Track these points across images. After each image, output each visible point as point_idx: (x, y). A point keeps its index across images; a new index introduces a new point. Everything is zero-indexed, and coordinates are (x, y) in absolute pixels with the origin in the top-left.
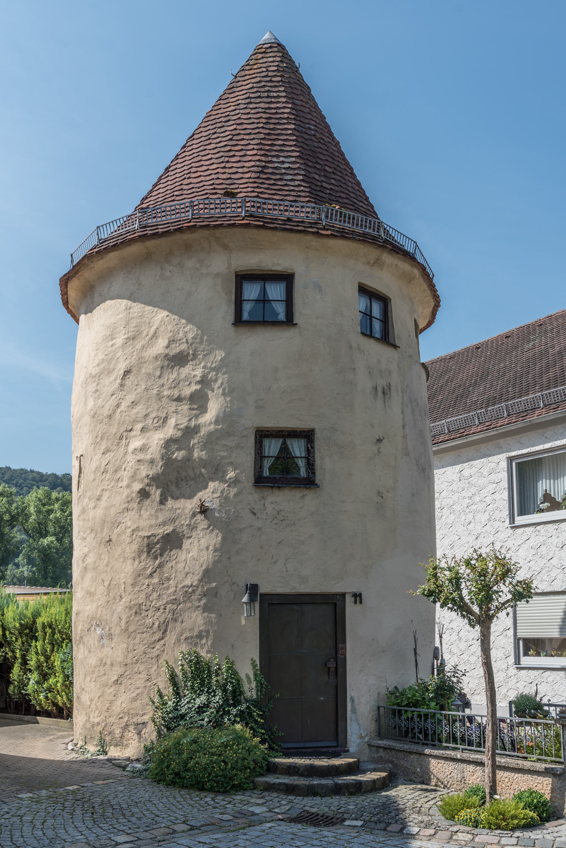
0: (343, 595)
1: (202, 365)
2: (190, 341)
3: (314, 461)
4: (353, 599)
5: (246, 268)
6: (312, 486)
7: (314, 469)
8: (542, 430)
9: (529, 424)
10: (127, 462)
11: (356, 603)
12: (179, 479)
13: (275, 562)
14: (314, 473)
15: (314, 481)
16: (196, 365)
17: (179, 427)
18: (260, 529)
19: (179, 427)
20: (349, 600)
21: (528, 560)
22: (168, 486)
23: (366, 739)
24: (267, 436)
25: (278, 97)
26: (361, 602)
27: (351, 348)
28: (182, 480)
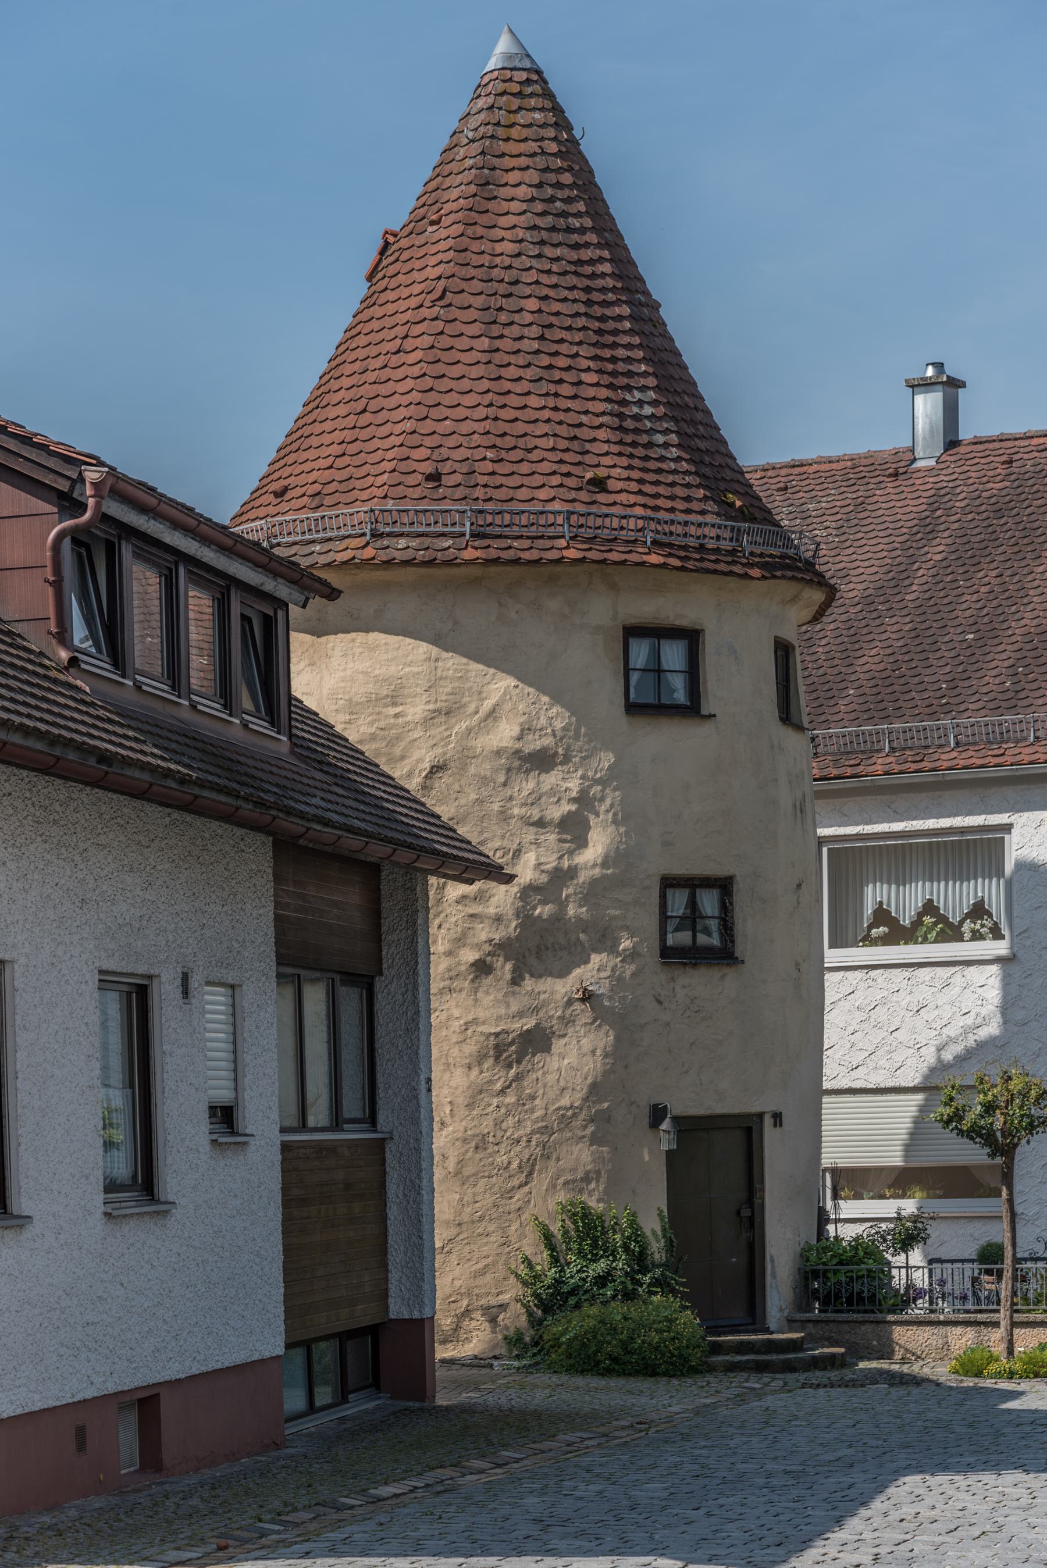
0: (761, 1116)
1: (580, 773)
2: (559, 734)
3: (733, 924)
4: (772, 1121)
5: (638, 621)
6: (732, 962)
7: (732, 936)
8: (887, 797)
9: (868, 784)
10: (443, 915)
11: (775, 1126)
12: (543, 947)
13: (686, 1072)
14: (733, 942)
15: (733, 953)
16: (569, 772)
17: (543, 867)
18: (668, 1024)
19: (543, 867)
20: (768, 1121)
21: (850, 1029)
22: (524, 957)
23: (786, 1314)
24: (672, 886)
25: (582, 230)
26: (781, 1125)
27: (772, 747)
28: (547, 949)
